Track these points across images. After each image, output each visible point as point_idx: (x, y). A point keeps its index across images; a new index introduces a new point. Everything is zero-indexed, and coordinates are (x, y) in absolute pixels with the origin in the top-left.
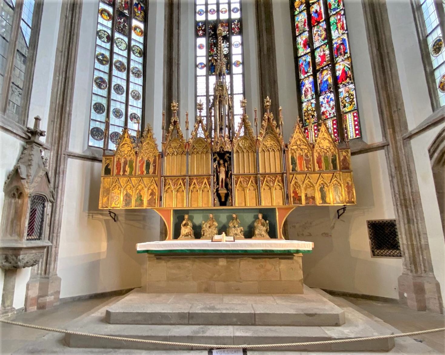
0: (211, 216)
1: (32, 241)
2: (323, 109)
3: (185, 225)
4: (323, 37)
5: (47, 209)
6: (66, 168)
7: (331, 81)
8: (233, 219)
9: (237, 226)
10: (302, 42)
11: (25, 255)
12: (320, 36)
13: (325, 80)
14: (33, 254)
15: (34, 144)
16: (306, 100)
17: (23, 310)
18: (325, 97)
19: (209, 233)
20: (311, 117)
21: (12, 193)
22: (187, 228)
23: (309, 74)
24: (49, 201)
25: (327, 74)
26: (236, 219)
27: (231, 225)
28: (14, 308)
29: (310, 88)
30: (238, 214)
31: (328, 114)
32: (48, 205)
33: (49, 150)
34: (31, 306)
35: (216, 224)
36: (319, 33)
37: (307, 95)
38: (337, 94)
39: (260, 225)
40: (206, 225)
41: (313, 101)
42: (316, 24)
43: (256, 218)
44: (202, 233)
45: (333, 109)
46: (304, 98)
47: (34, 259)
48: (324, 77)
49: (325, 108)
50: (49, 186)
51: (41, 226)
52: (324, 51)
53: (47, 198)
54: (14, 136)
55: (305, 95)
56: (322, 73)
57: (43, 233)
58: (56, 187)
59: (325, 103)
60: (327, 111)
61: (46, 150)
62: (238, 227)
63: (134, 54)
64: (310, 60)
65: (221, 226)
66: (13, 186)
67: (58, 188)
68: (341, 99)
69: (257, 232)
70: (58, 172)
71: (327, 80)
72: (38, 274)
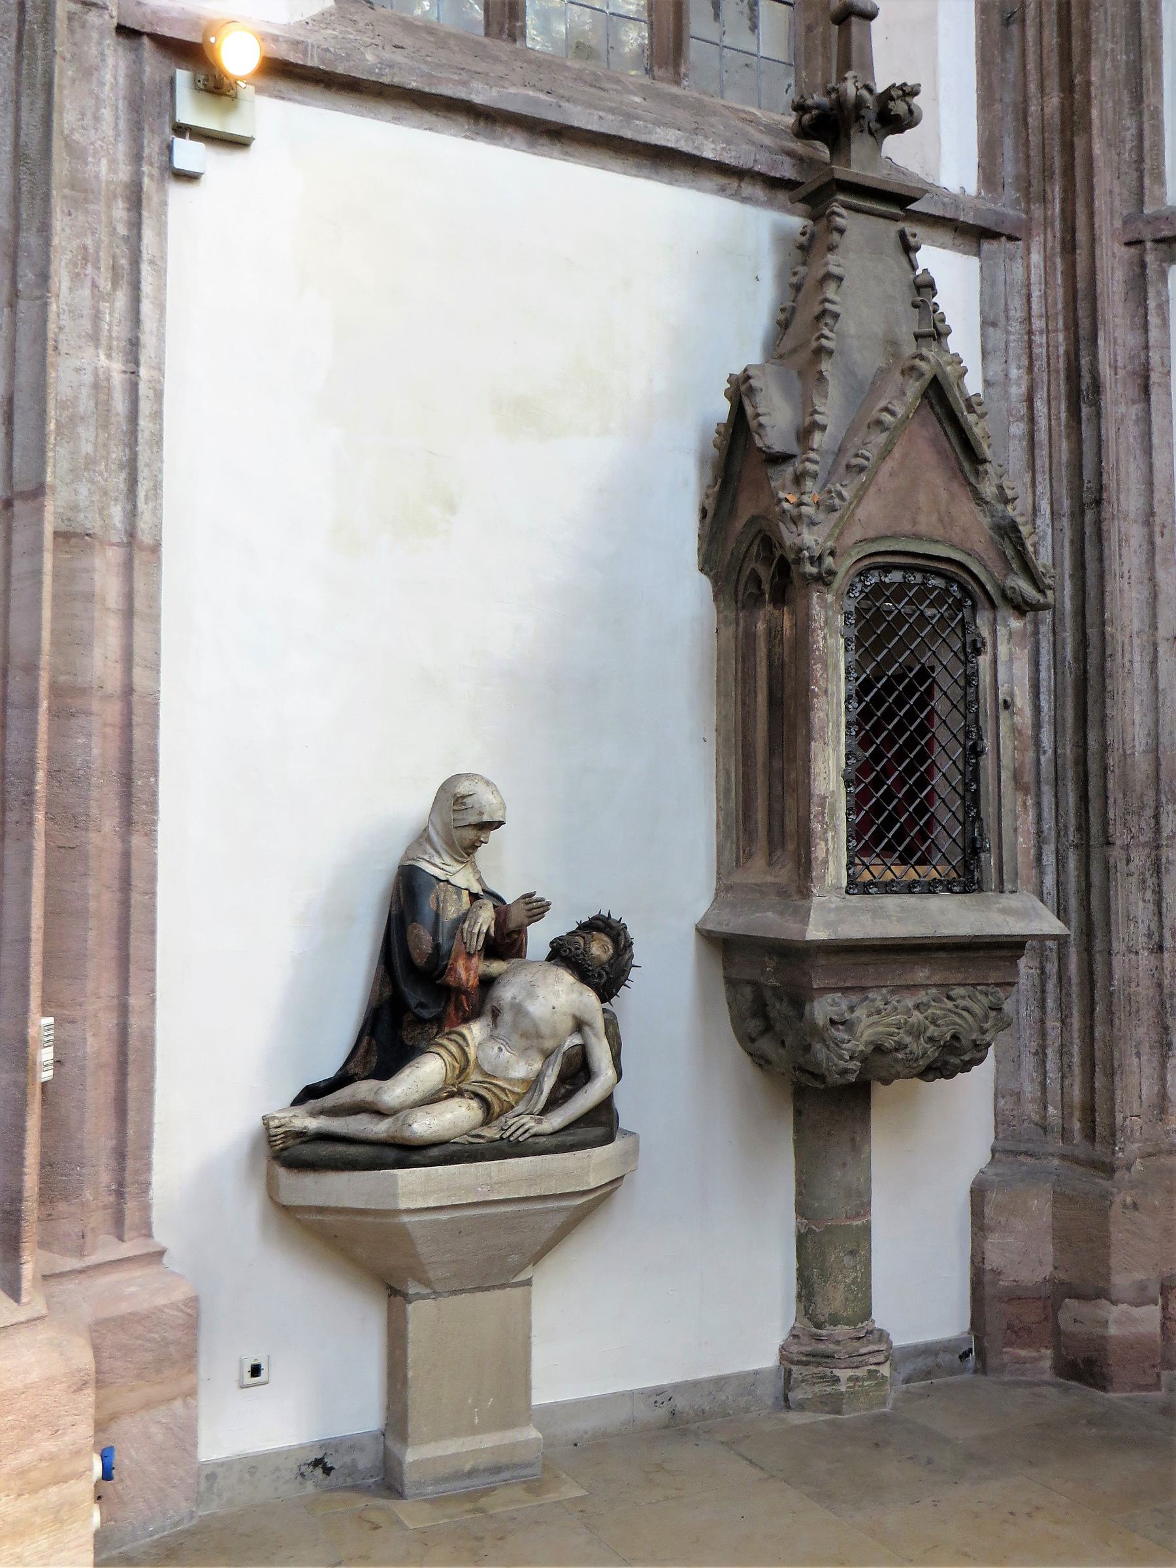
1: (891, 902)
5: (995, 661)
6: (1166, 346)
11: (854, 998)
14: (922, 996)
15: (841, 197)
17: (965, 1356)
21: (746, 572)
24: (997, 600)
28: (882, 1336)
32: (1002, 631)
33: (1011, 238)
34: (1010, 1344)
47: (932, 1030)
50: (988, 489)
51: (972, 799)
53: (983, 578)
54: (722, 191)
57: (991, 842)
58: (1088, 497)
61: (987, 246)
66: (739, 524)
67: (1098, 502)
70: (1086, 381)
72: (1045, 1129)
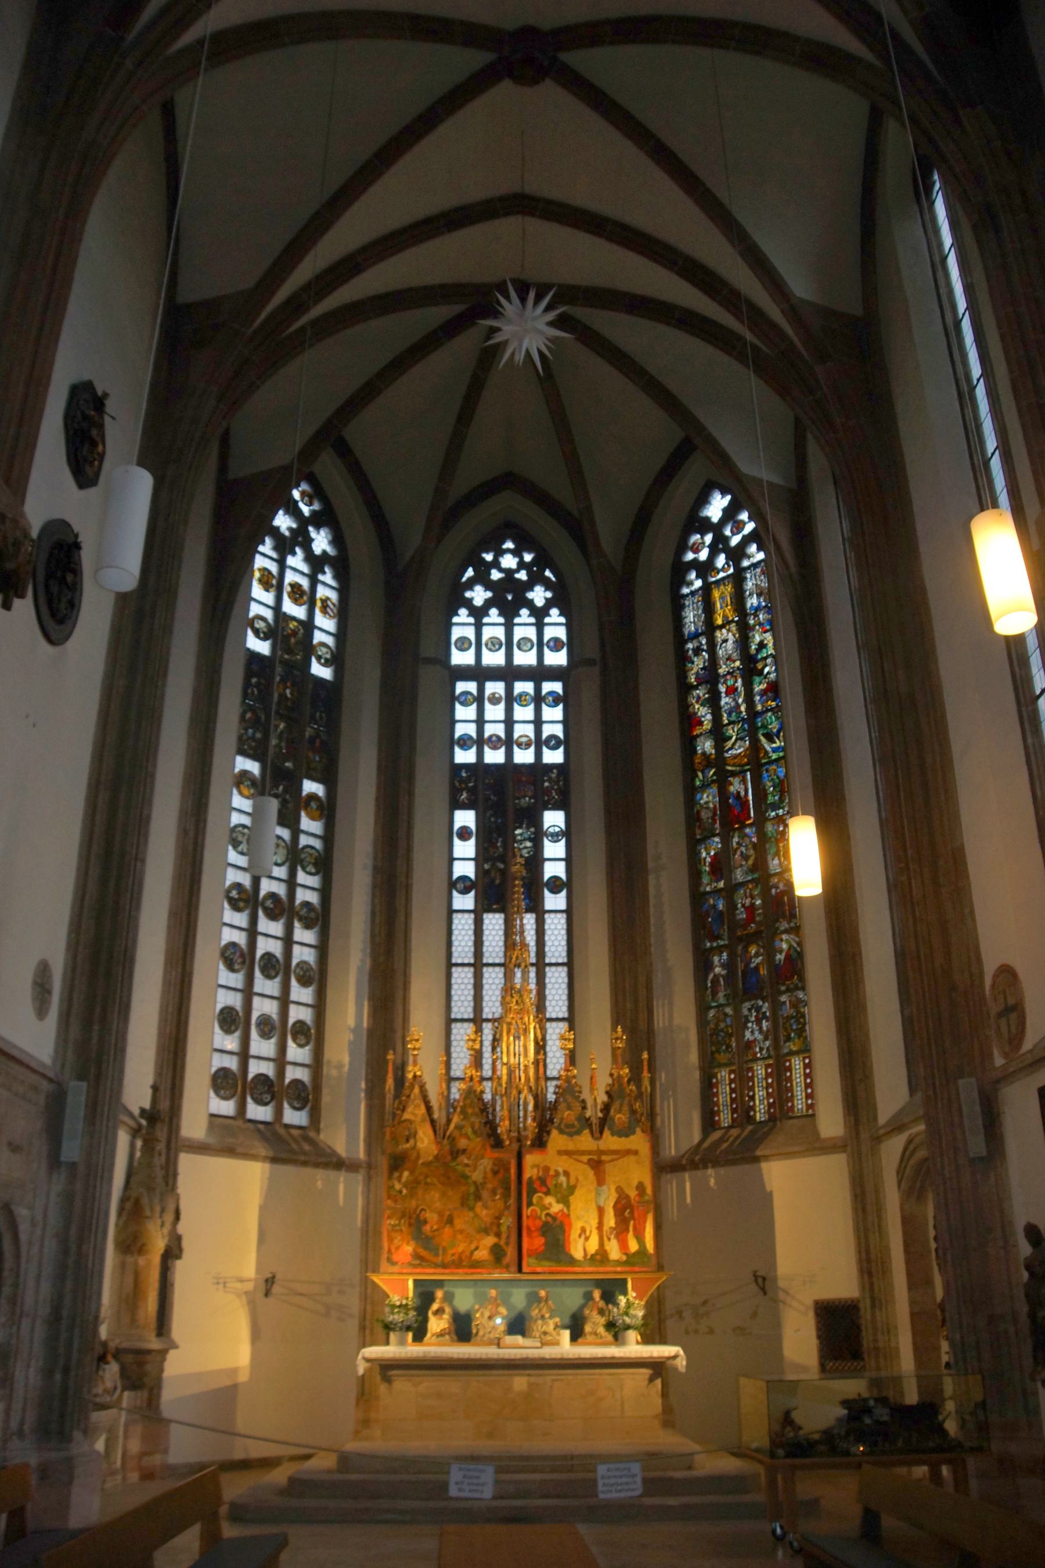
0: (493, 1293)
2: (748, 1035)
3: (439, 1312)
4: (750, 862)
7: (763, 971)
8: (539, 1300)
9: (547, 1315)
10: (709, 860)
12: (746, 857)
13: (753, 965)
16: (714, 1004)
18: (752, 1006)
19: (489, 1330)
20: (724, 1047)
22: (441, 1318)
23: (721, 943)
25: (757, 955)
26: (546, 1301)
27: (535, 1313)
29: (722, 976)
30: (548, 1289)
31: (758, 1050)
35: (503, 1310)
36: (743, 849)
37: (717, 994)
38: (776, 1006)
39: (595, 1313)
40: (482, 1314)
41: (729, 1010)
42: (737, 826)
43: (588, 1296)
44: (474, 1331)
45: (766, 1039)
46: (710, 997)
48: (751, 958)
49: (752, 1032)
52: (752, 897)
55: (712, 991)
56: (746, 949)
59: (753, 1022)
60: (755, 1040)
62: (551, 1317)
63: (304, 869)
64: (725, 910)
65: (513, 1314)
68: (783, 1018)
69: (588, 1328)
71: (757, 968)
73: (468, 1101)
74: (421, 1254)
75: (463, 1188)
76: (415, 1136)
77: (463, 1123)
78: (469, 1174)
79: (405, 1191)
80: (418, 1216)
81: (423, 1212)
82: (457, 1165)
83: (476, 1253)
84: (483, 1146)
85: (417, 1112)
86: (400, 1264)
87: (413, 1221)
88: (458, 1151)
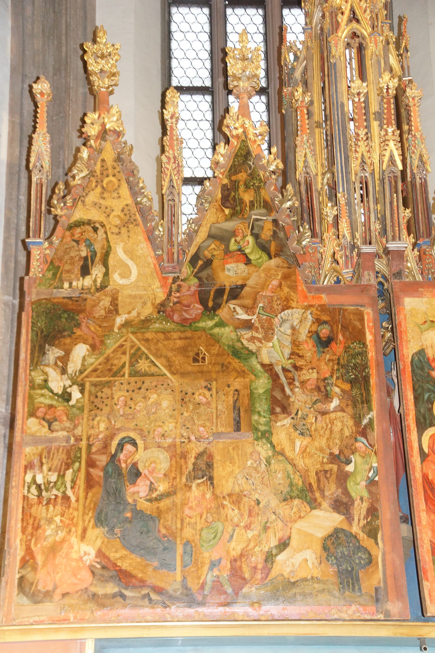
73: (242, 176)
74: (125, 565)
75: (237, 384)
76: (105, 264)
77: (230, 225)
78: (252, 347)
79: (76, 395)
80: (114, 457)
81: (129, 447)
82: (221, 324)
83: (281, 558)
84: (286, 277)
85: (109, 202)
86: (57, 597)
87: (97, 473)
88: (220, 292)
